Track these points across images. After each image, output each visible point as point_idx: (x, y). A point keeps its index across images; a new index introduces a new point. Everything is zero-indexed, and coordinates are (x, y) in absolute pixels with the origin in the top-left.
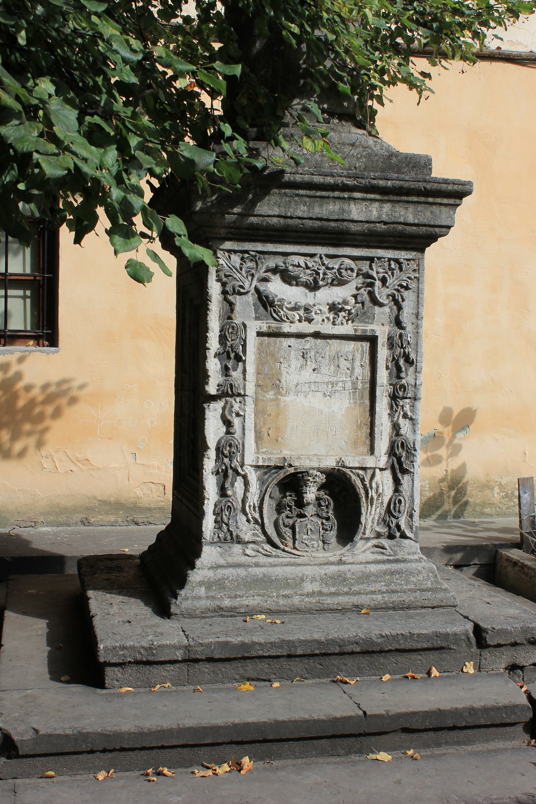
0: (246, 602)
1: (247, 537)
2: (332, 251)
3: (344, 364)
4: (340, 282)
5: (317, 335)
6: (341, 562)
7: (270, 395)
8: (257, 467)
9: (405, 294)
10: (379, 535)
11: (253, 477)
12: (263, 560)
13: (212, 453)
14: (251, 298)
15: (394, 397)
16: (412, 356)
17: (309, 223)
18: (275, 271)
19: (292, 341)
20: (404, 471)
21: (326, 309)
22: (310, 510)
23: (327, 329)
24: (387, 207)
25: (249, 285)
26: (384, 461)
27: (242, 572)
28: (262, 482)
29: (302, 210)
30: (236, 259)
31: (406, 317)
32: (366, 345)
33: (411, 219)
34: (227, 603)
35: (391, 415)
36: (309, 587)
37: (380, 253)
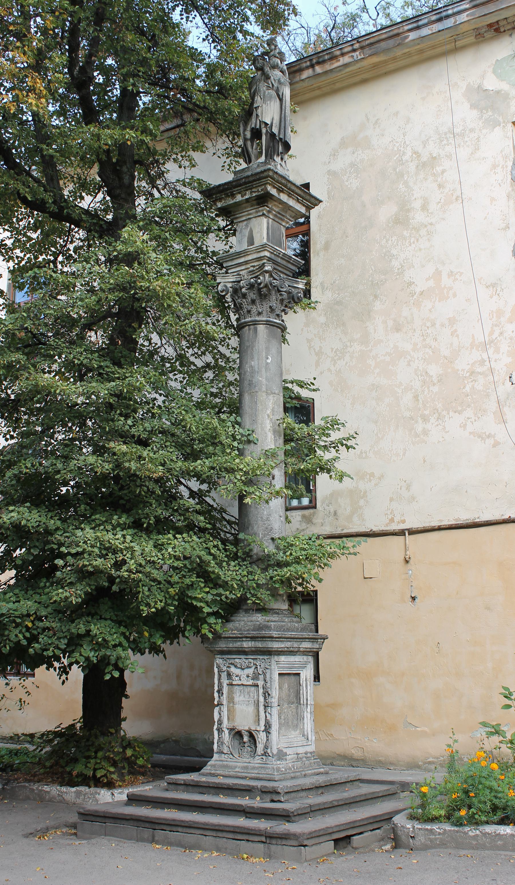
0: (217, 772)
1: (225, 752)
2: (246, 657)
3: (252, 695)
4: (248, 667)
5: (243, 685)
6: (249, 763)
7: (232, 705)
8: (228, 729)
9: (267, 670)
10: (262, 755)
11: (227, 732)
12: (229, 760)
13: (216, 723)
14: (225, 673)
15: (265, 707)
16: (270, 693)
17: (234, 649)
18: (231, 664)
19: (237, 687)
20: (269, 733)
21: (245, 676)
22: (246, 745)
23: (245, 683)
24: (253, 642)
25: (225, 668)
26: (263, 728)
27: (221, 763)
28: (230, 734)
29: (231, 645)
30: (221, 660)
31: (268, 679)
32: (256, 688)
33: (260, 646)
34: (213, 772)
35: (265, 712)
36: (237, 770)
37: (259, 657)
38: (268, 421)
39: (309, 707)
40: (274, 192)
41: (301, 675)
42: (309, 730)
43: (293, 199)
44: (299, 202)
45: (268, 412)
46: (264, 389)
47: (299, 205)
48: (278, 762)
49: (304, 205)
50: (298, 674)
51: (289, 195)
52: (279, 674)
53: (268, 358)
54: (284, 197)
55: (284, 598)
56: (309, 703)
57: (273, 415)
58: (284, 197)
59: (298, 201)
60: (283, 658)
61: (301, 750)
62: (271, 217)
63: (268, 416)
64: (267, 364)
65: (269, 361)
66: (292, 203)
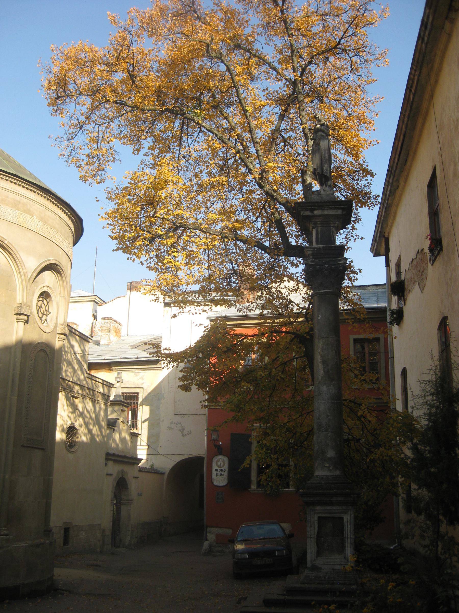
38: (319, 357)
39: (349, 540)
40: (308, 213)
41: (344, 518)
42: (349, 554)
43: (327, 209)
44: (334, 209)
45: (319, 351)
46: (317, 337)
47: (335, 210)
48: (311, 573)
49: (339, 209)
50: (343, 518)
51: (323, 209)
52: (319, 518)
53: (318, 316)
54: (316, 212)
55: (331, 468)
56: (349, 536)
57: (322, 351)
58: (316, 212)
59: (331, 209)
60: (318, 507)
61: (337, 567)
62: (319, 226)
63: (319, 353)
64: (318, 319)
65: (319, 318)
66: (326, 212)
